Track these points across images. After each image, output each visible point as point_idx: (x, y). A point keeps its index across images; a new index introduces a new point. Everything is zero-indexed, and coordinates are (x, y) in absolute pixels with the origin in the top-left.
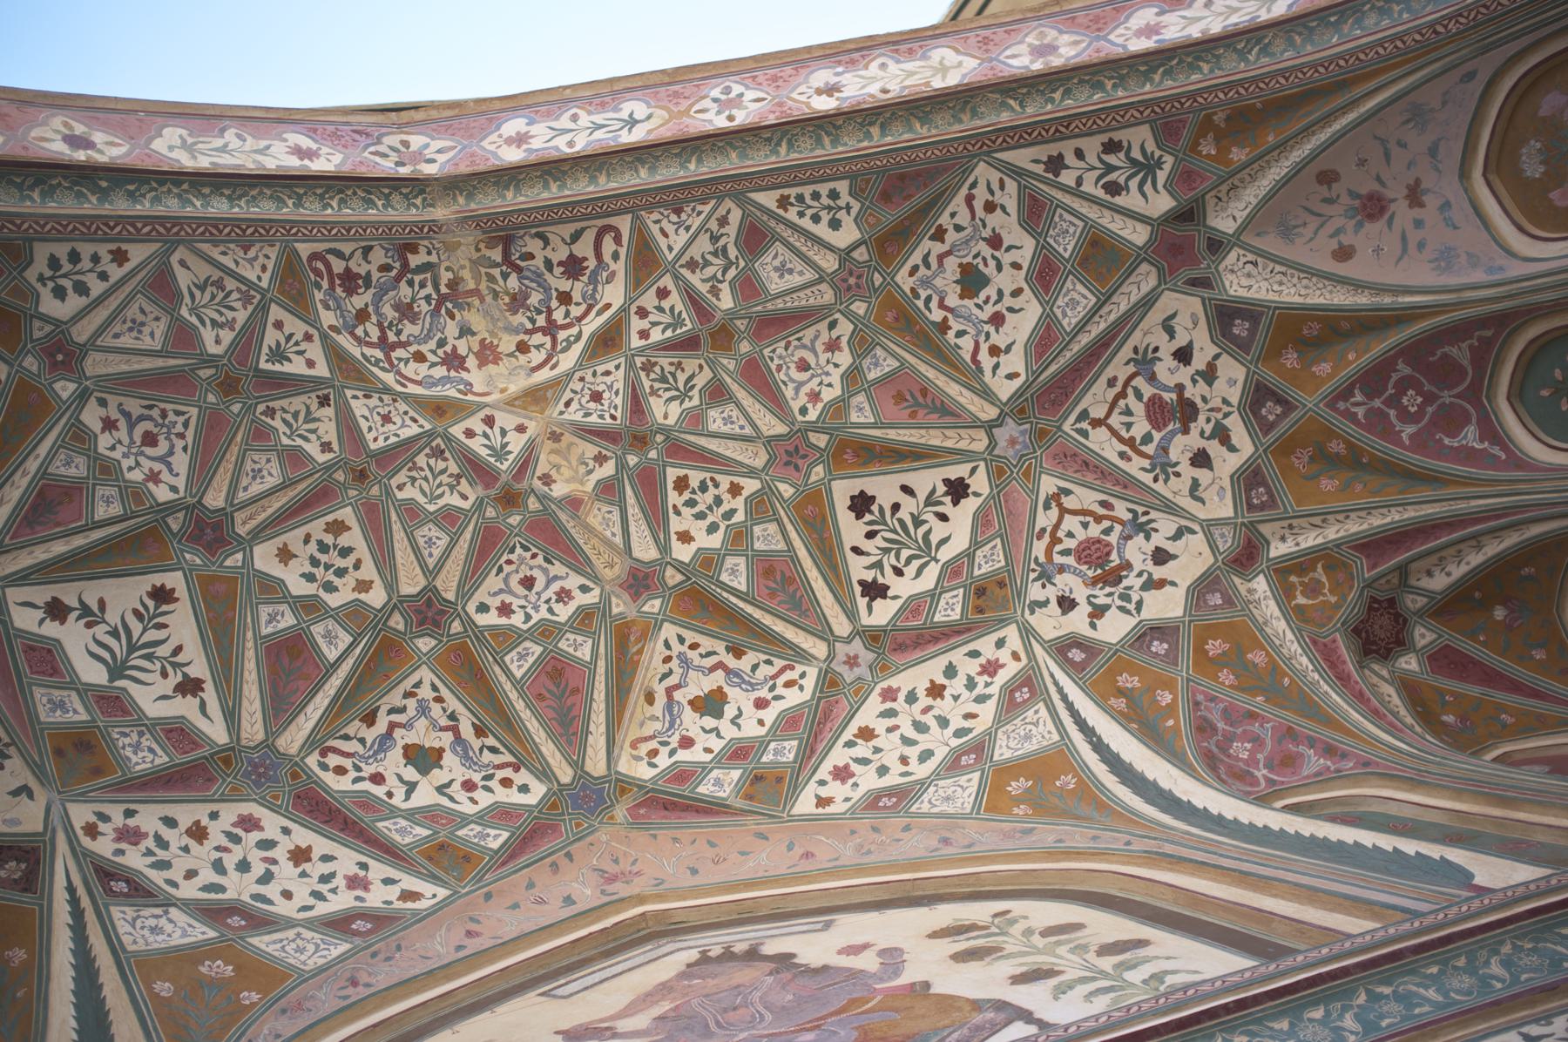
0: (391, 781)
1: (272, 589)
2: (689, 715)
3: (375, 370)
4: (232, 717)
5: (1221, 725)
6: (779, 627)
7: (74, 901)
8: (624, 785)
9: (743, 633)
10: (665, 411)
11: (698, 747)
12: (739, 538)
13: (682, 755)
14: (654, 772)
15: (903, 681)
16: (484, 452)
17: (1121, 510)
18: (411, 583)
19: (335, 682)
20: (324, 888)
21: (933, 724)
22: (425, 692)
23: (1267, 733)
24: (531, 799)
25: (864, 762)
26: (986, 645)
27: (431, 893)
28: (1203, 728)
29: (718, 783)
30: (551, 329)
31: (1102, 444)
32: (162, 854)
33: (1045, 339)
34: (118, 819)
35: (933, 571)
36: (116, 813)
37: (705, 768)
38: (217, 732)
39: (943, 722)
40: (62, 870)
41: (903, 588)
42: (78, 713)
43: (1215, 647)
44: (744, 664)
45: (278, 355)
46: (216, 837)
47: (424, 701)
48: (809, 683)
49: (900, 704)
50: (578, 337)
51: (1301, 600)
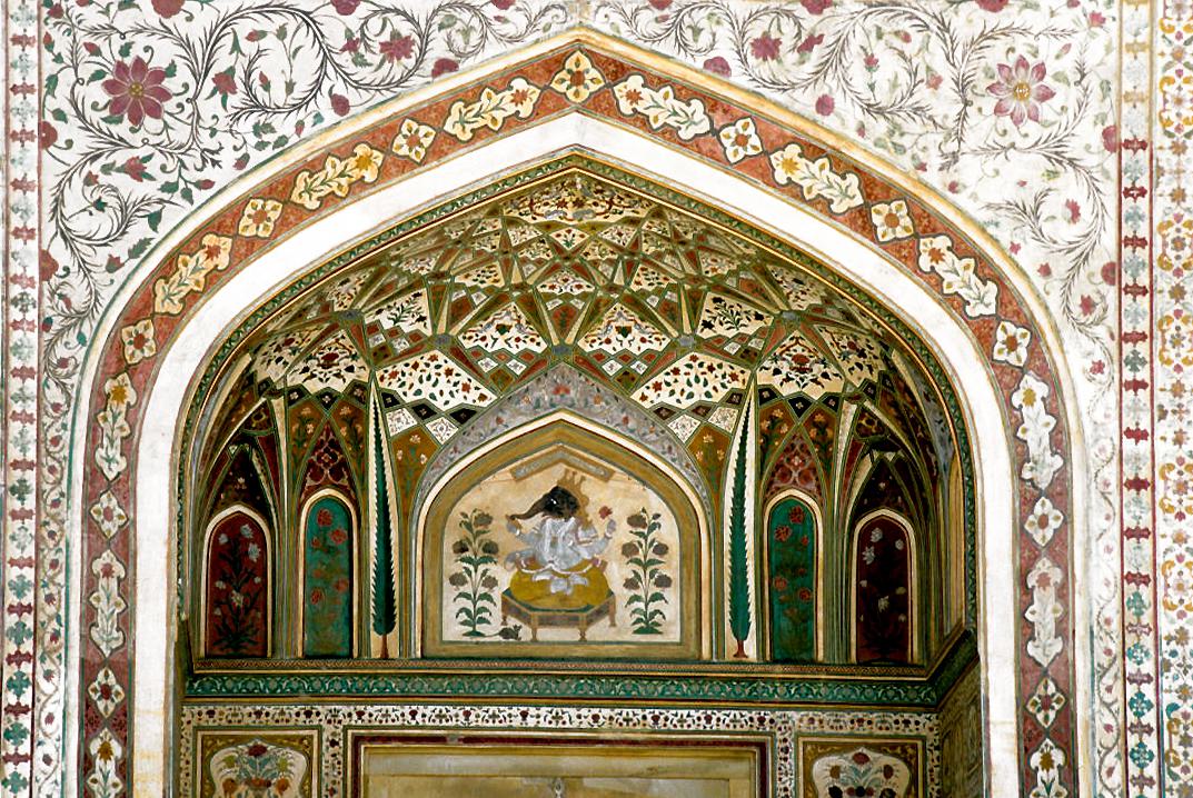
0: (489, 338)
1: (460, 286)
2: (614, 331)
3: (524, 218)
4: (434, 327)
5: (797, 448)
6: (666, 325)
7: (375, 408)
8: (576, 348)
9: (646, 315)
10: (648, 248)
11: (611, 346)
12: (659, 292)
13: (604, 347)
14: (590, 349)
15: (702, 357)
16: (562, 243)
17: (821, 356)
18: (516, 279)
19: (476, 310)
20: (454, 389)
21: (702, 381)
22: (511, 309)
23: (809, 462)
24: (539, 350)
25: (668, 384)
26: (737, 369)
27: (492, 397)
28: (790, 449)
29: (611, 367)
30: (611, 203)
31: (828, 340)
32: (403, 379)
33: (816, 309)
34: (390, 369)
35: (734, 332)
36: (390, 369)
37: (610, 357)
38: (428, 332)
39: (706, 384)
40: (373, 397)
41: (720, 330)
42: (381, 339)
43: (819, 418)
44: (644, 324)
45: (483, 229)
46: (422, 366)
47: (509, 314)
48: (665, 344)
49: (695, 365)
50: (621, 213)
51: (863, 422)
